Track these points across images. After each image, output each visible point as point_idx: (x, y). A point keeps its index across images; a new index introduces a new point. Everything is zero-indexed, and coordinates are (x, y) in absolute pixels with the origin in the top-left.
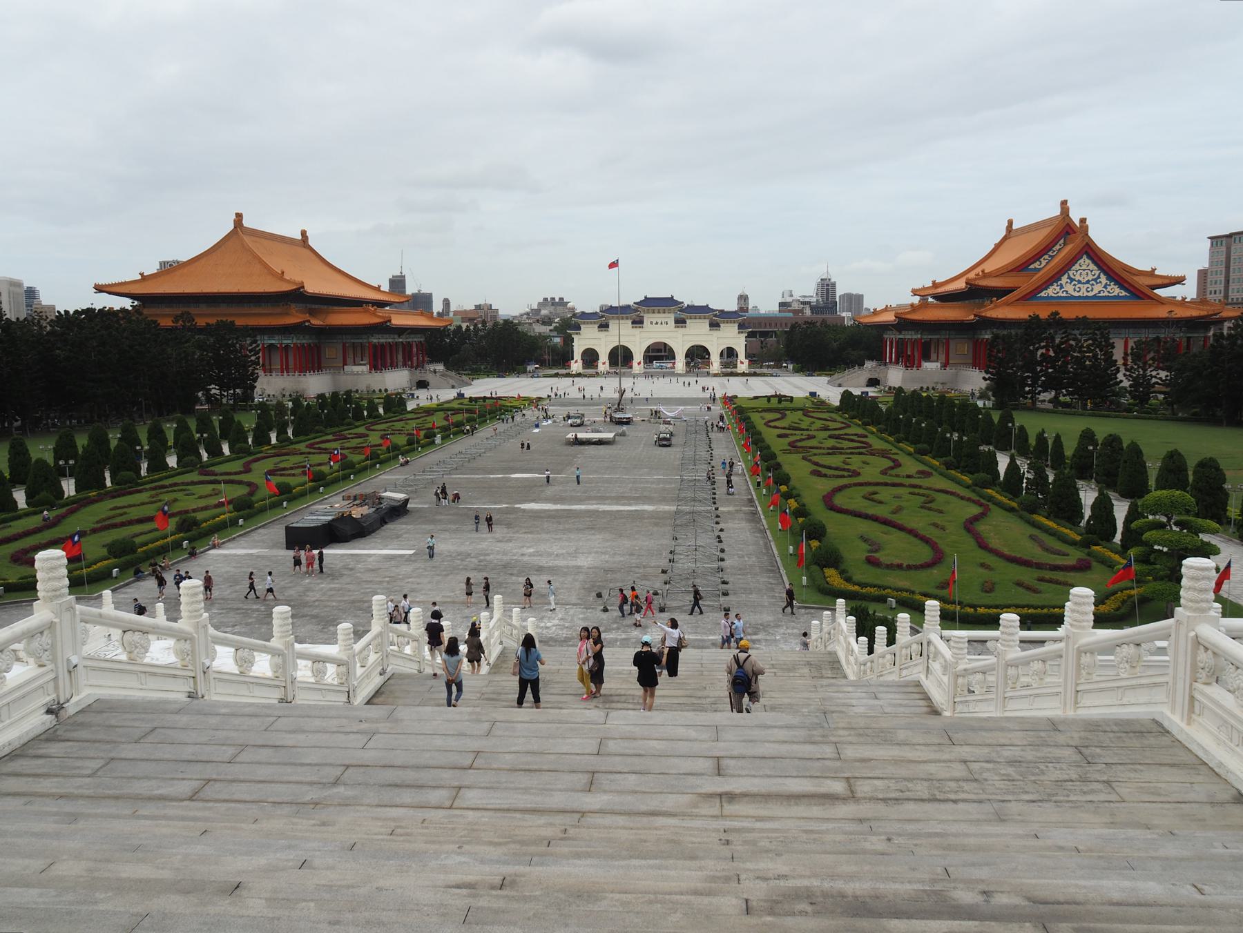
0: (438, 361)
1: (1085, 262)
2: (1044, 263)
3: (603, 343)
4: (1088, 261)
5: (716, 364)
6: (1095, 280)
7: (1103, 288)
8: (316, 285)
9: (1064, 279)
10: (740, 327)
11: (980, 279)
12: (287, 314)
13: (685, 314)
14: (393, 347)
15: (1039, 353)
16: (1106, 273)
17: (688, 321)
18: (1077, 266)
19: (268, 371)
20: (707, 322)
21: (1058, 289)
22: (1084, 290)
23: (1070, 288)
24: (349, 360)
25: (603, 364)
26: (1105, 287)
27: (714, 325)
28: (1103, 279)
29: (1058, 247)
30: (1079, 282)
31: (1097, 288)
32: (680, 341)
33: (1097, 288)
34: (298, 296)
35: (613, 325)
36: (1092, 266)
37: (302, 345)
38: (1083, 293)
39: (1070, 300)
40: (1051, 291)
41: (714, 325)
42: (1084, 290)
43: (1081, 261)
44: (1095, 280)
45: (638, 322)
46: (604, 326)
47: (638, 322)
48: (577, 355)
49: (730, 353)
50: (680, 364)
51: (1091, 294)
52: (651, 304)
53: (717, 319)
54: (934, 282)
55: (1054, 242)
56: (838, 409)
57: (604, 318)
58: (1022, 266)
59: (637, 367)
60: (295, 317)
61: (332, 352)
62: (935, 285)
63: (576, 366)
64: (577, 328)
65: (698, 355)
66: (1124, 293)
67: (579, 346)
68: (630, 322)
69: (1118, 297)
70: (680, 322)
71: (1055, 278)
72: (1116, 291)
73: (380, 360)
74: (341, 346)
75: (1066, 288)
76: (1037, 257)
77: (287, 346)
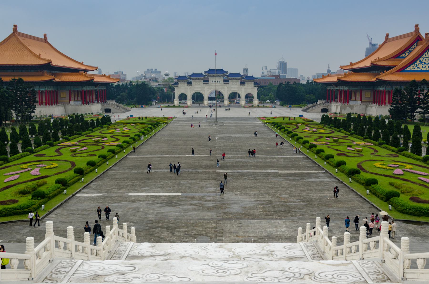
0: (112, 99)
2: (407, 54)
3: (189, 92)
5: (243, 102)
8: (55, 63)
9: (418, 62)
10: (256, 84)
11: (377, 61)
12: (42, 75)
13: (229, 78)
14: (90, 92)
15: (415, 97)
17: (230, 81)
18: (424, 56)
19: (41, 103)
20: (239, 81)
21: (415, 66)
23: (420, 66)
24: (72, 99)
25: (189, 102)
27: (243, 83)
29: (413, 47)
30: (425, 63)
32: (226, 91)
34: (48, 67)
35: (194, 83)
37: (50, 91)
41: (243, 83)
42: (427, 67)
43: (426, 53)
45: (206, 82)
46: (190, 83)
47: (206, 82)
48: (177, 96)
49: (249, 97)
50: (226, 102)
52: (212, 73)
53: (244, 79)
54: (351, 63)
55: (412, 44)
56: (321, 124)
57: (189, 80)
58: (397, 56)
59: (206, 102)
60: (47, 78)
61: (64, 95)
62: (351, 64)
63: (176, 102)
64: (177, 84)
65: (233, 96)
67: (178, 92)
68: (202, 81)
70: (226, 82)
71: (413, 61)
73: (85, 99)
74: (68, 92)
76: (404, 51)
77: (42, 92)
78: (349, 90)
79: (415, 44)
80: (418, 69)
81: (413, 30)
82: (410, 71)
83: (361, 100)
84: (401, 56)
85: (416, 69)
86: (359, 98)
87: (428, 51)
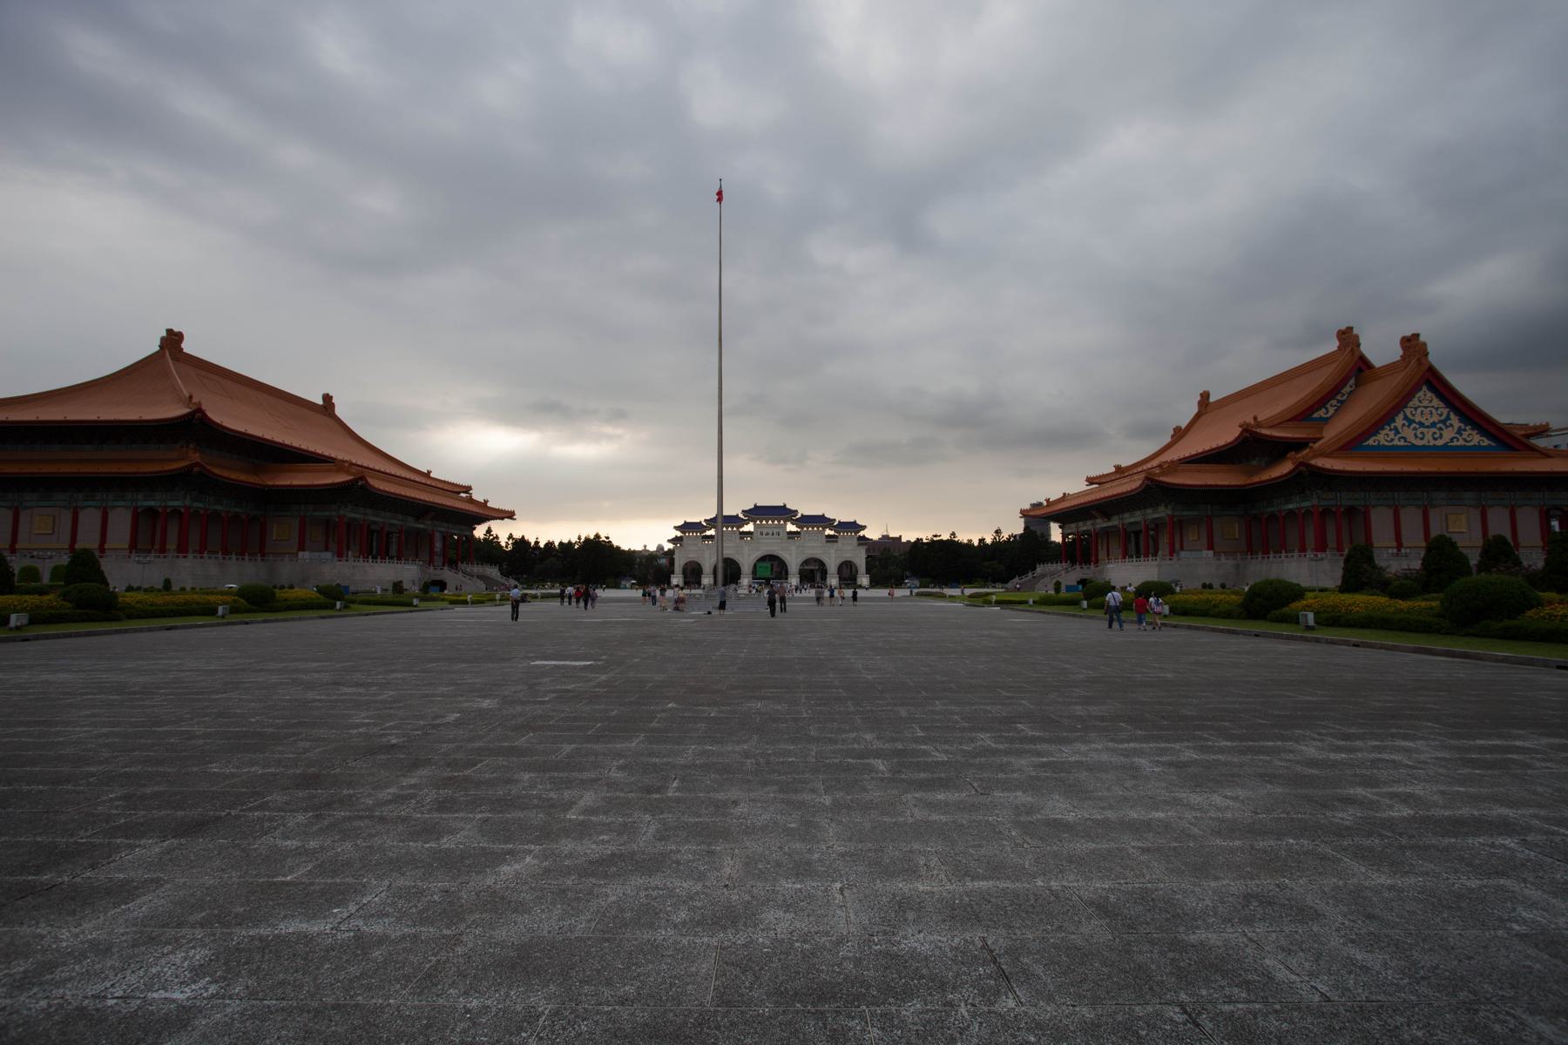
1: (1425, 396)
2: (1331, 411)
4: (1429, 394)
6: (1443, 422)
7: (1454, 433)
16: (1458, 412)
21: (1392, 435)
22: (1429, 437)
23: (1408, 433)
26: (1459, 432)
28: (1455, 421)
29: (1347, 389)
30: (1421, 424)
31: (1448, 435)
33: (1448, 435)
36: (1436, 402)
38: (1428, 440)
39: (1411, 451)
40: (1383, 437)
42: (1429, 437)
43: (1420, 394)
44: (1443, 422)
51: (1440, 443)
58: (1304, 415)
66: (1486, 442)
69: (1478, 447)
71: (1384, 419)
72: (1476, 439)
75: (1399, 434)
76: (1322, 402)
78: (1171, 517)
79: (1352, 381)
80: (1402, 443)
81: (1333, 345)
82: (1380, 447)
83: (1210, 547)
84: (1315, 415)
85: (1396, 442)
86: (1204, 541)
87: (1425, 388)
